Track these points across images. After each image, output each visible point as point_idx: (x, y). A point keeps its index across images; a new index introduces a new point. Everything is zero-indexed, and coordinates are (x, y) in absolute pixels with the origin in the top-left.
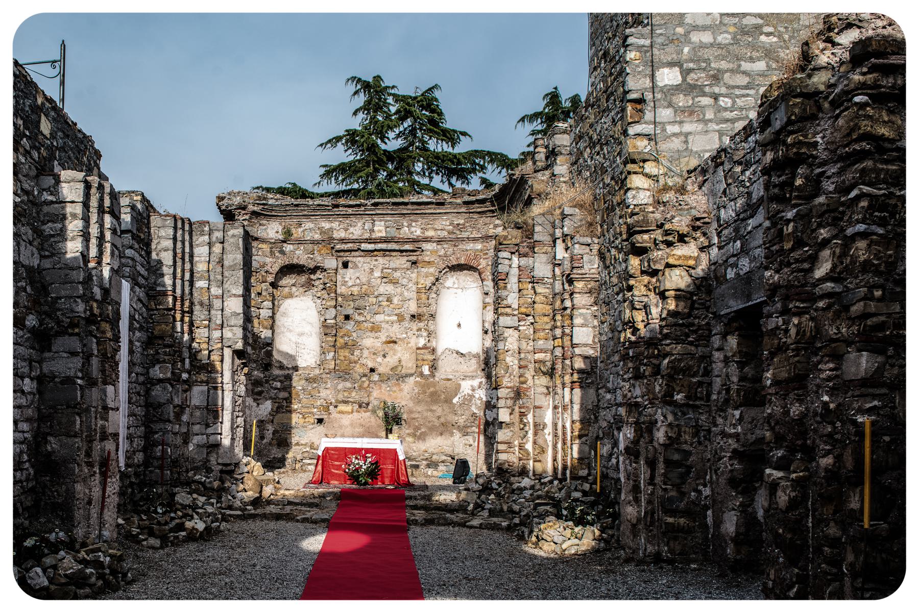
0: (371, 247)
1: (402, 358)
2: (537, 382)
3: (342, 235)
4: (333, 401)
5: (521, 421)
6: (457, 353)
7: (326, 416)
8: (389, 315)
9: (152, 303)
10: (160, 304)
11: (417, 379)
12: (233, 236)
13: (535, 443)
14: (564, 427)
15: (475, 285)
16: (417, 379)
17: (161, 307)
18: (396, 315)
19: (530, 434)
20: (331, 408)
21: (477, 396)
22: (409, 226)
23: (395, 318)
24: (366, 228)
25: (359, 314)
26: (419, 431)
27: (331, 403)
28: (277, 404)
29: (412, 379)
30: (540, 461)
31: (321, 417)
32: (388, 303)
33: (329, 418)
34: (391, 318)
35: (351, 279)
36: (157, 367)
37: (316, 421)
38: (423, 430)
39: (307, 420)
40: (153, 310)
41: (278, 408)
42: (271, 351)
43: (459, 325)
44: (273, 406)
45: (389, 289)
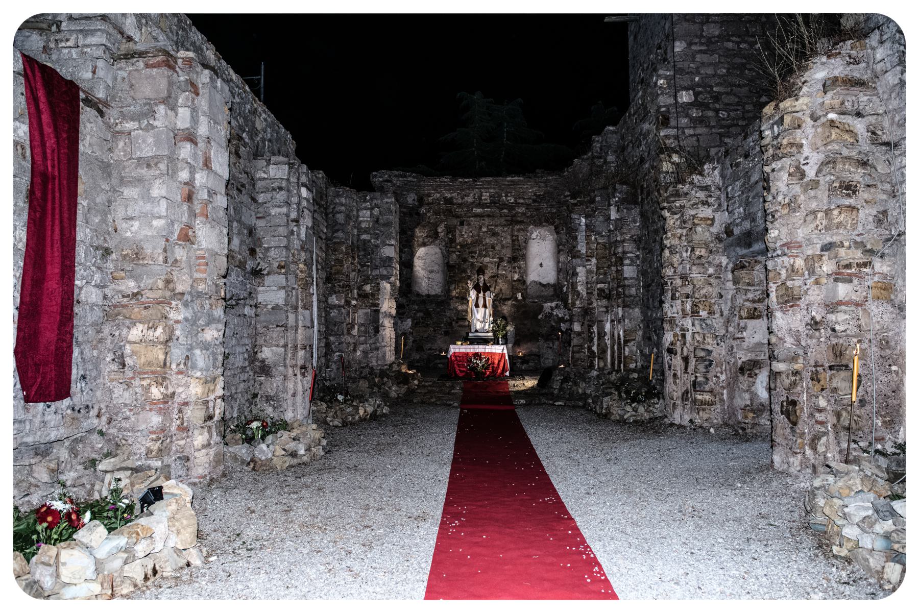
0: (479, 210)
1: (503, 288)
3: (460, 201)
5: (589, 330)
6: (540, 284)
8: (493, 258)
12: (387, 203)
14: (619, 335)
21: (555, 313)
22: (506, 196)
27: (454, 320)
29: (510, 302)
44: (412, 322)
45: (493, 240)
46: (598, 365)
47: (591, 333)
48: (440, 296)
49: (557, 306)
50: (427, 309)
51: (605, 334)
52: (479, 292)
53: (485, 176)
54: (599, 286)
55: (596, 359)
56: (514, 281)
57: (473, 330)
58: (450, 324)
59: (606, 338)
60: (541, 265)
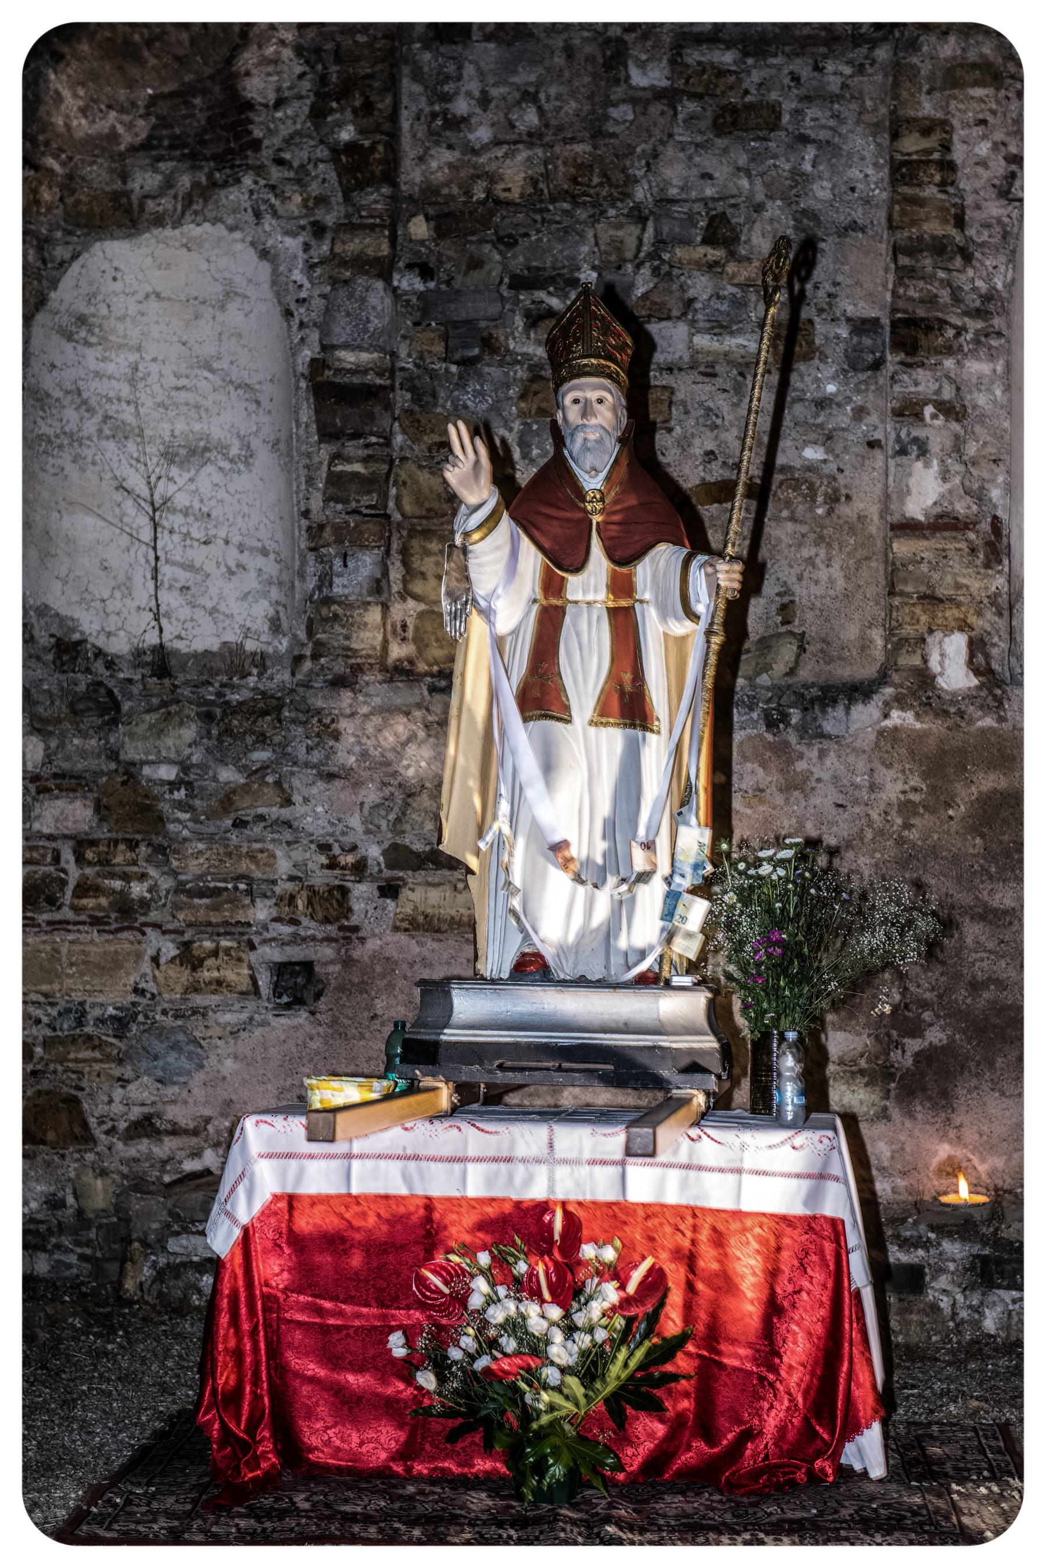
4: (374, 852)
7: (327, 952)
8: (719, 327)
11: (897, 717)
16: (897, 717)
26: (914, 1045)
27: (360, 868)
31: (296, 953)
32: (716, 254)
33: (348, 962)
34: (731, 343)
35: (484, 101)
38: (936, 1036)
39: (206, 975)
48: (261, 661)
50: (130, 772)
56: (908, 528)
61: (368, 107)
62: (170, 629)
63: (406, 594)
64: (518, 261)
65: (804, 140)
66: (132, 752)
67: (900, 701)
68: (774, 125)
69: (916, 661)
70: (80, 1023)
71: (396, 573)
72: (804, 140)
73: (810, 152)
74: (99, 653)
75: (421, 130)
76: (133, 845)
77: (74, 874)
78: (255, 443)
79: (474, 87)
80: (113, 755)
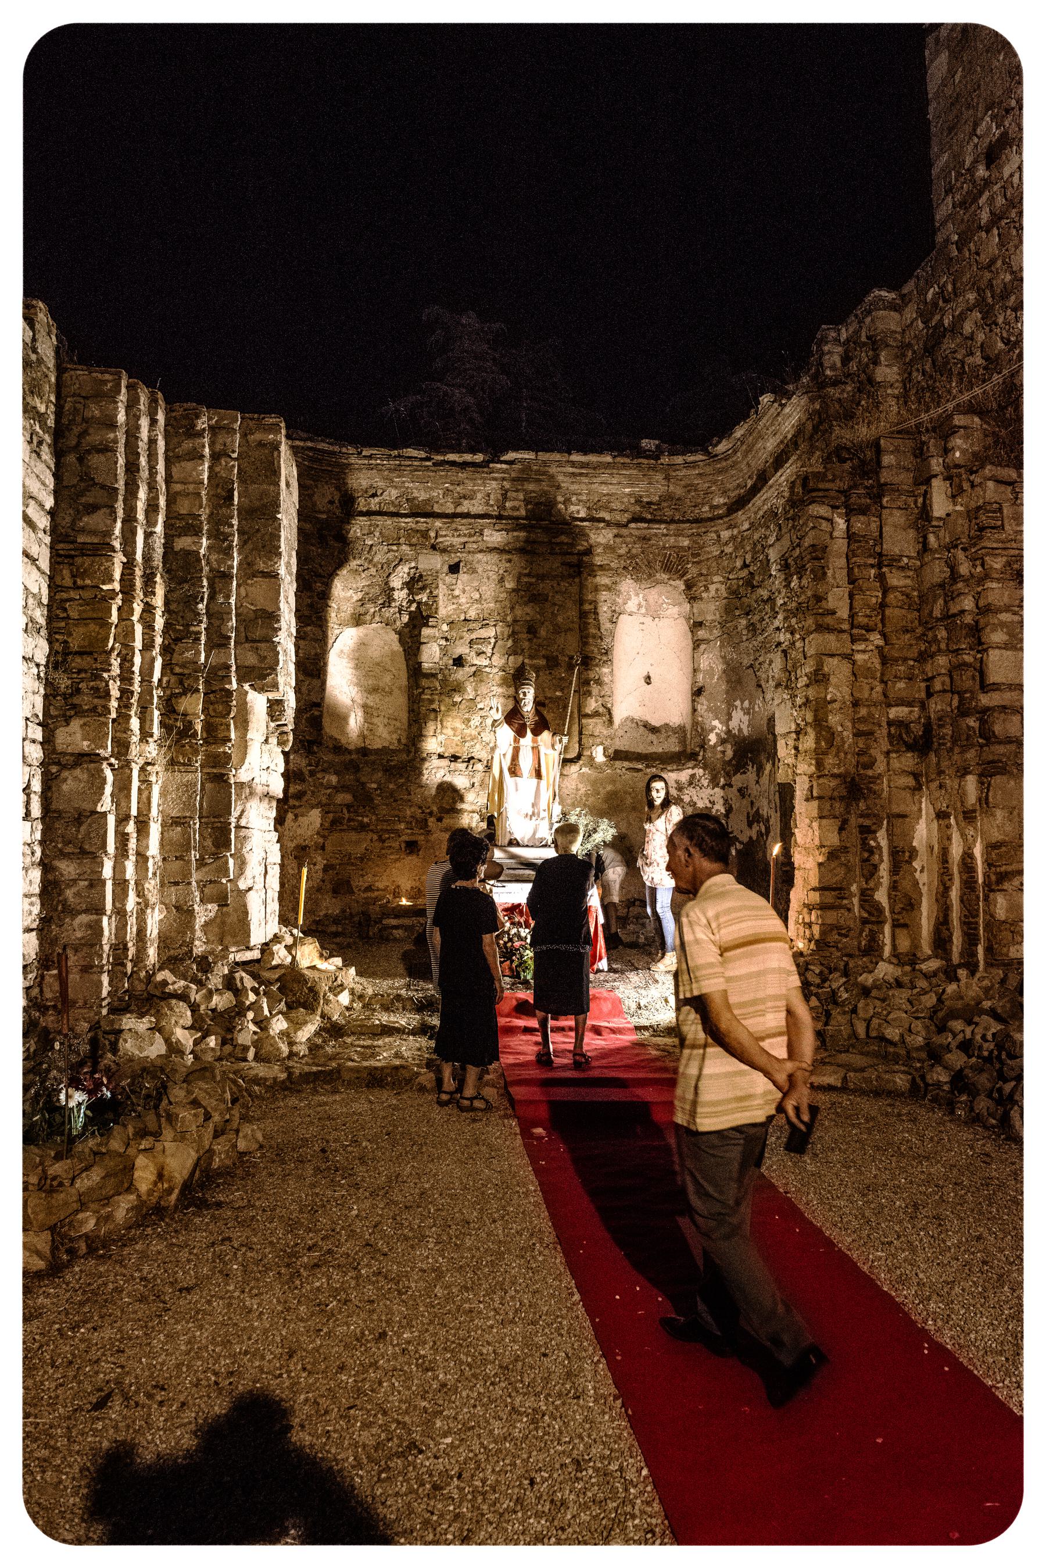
2: (896, 764)
4: (435, 809)
5: (864, 843)
6: (646, 725)
7: (422, 838)
9: (66, 572)
10: (84, 575)
11: (584, 770)
13: (894, 887)
15: (674, 611)
17: (88, 582)
18: (544, 657)
19: (884, 870)
20: (431, 821)
23: (542, 662)
24: (492, 502)
25: (478, 654)
27: (431, 814)
28: (331, 815)
30: (905, 926)
31: (413, 838)
32: (530, 636)
35: (464, 592)
36: (76, 724)
37: (403, 845)
40: (68, 589)
41: (333, 823)
42: (321, 716)
43: (648, 680)
46: (894, 946)
47: (871, 851)
49: (692, 781)
51: (913, 853)
52: (520, 732)
53: (516, 449)
54: (894, 713)
55: (887, 929)
57: (502, 840)
58: (423, 824)
59: (916, 864)
60: (648, 680)
61: (431, 592)
62: (367, 742)
63: (441, 733)
64: (474, 636)
65: (555, 604)
66: (363, 779)
67: (584, 765)
68: (546, 600)
69: (589, 753)
70: (350, 859)
71: (439, 726)
72: (555, 604)
73: (557, 608)
74: (346, 749)
75: (445, 599)
76: (364, 807)
77: (347, 816)
78: (394, 688)
79: (461, 587)
80: (358, 780)
